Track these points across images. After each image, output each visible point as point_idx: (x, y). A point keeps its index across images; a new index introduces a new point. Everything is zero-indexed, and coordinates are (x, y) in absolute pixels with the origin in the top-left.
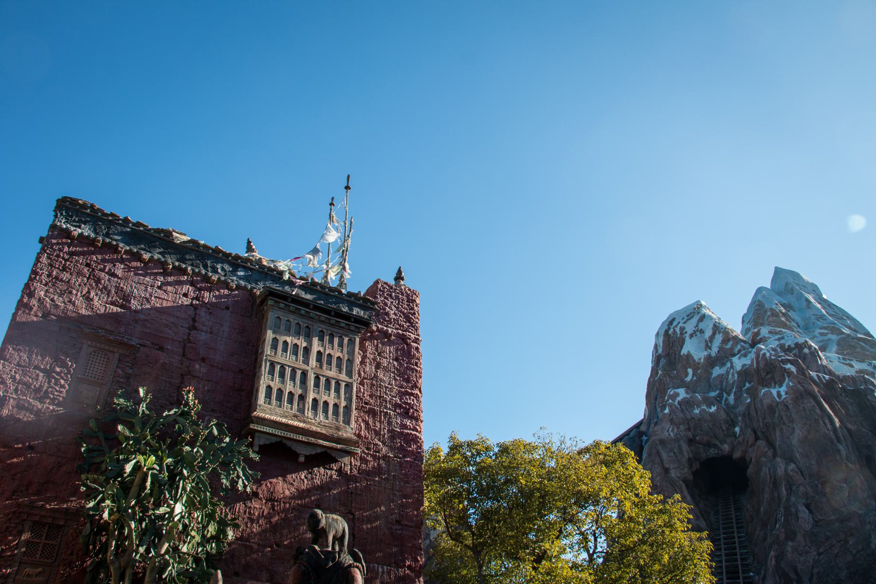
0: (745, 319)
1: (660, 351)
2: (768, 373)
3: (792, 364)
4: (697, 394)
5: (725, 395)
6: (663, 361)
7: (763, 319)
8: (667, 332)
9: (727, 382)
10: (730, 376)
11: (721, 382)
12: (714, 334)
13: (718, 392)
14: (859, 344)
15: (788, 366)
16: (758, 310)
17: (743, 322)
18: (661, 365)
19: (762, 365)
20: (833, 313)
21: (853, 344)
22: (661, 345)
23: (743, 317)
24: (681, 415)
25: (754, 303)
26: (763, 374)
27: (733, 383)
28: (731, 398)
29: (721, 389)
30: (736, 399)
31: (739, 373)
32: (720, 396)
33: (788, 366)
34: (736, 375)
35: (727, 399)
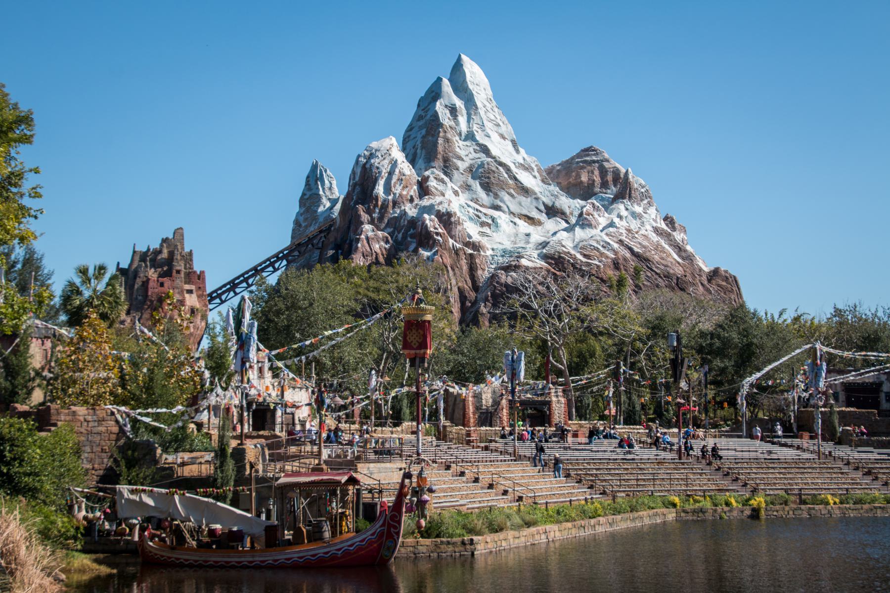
0: (421, 103)
1: (357, 179)
2: (426, 239)
3: (441, 236)
4: (379, 232)
5: (396, 233)
6: (358, 189)
7: (435, 131)
8: (365, 164)
9: (399, 224)
10: (402, 221)
11: (396, 223)
12: (398, 180)
13: (392, 229)
14: (497, 168)
15: (439, 238)
16: (433, 120)
17: (419, 105)
18: (356, 192)
19: (423, 232)
20: (493, 118)
21: (494, 169)
22: (359, 174)
23: (420, 101)
24: (368, 249)
25: (433, 92)
26: (423, 239)
27: (404, 225)
28: (400, 236)
29: (395, 228)
30: (403, 238)
31: (409, 221)
32: (393, 232)
33: (439, 238)
34: (406, 222)
35: (397, 236)
